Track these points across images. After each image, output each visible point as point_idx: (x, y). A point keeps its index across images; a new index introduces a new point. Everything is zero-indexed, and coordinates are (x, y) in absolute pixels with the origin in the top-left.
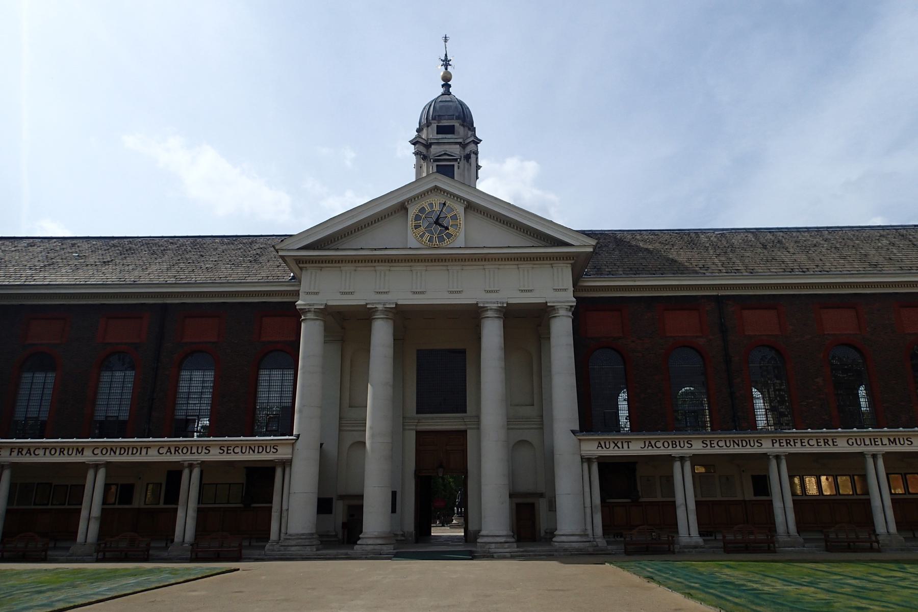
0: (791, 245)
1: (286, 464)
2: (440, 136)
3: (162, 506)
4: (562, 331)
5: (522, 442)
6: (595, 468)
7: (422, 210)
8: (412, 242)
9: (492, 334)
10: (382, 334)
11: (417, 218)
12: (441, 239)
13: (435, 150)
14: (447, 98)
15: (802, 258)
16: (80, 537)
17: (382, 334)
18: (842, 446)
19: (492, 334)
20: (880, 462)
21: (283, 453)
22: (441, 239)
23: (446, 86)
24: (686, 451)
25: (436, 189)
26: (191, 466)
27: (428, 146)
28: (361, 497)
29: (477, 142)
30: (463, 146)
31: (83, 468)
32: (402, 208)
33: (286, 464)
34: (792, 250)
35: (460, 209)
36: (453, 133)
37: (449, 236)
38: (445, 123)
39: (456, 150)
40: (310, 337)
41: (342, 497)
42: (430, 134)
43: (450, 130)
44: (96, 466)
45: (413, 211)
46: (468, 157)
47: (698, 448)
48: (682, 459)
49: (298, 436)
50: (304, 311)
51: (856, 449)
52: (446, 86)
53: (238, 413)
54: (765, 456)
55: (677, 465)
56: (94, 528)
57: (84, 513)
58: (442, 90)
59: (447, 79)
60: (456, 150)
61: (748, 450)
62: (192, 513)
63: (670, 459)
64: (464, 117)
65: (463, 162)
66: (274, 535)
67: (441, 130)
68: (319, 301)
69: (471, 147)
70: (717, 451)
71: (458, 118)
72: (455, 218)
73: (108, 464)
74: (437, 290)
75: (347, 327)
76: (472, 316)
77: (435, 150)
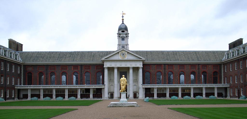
0: (178, 54)
1: (104, 88)
2: (122, 33)
3: (85, 93)
4: (141, 71)
5: (135, 85)
6: (144, 89)
7: (121, 53)
9: (131, 71)
11: (120, 54)
12: (124, 58)
13: (121, 35)
14: (123, 25)
15: (179, 57)
19: (131, 71)
20: (181, 88)
21: (103, 87)
22: (124, 58)
23: (123, 22)
26: (91, 88)
28: (114, 92)
29: (128, 34)
30: (126, 35)
31: (77, 89)
32: (118, 53)
33: (104, 88)
34: (178, 56)
35: (127, 53)
36: (124, 32)
37: (125, 57)
39: (125, 36)
40: (106, 72)
41: (110, 92)
42: (120, 32)
43: (123, 32)
45: (120, 53)
46: (127, 37)
47: (157, 87)
49: (105, 85)
50: (105, 68)
52: (123, 22)
54: (166, 88)
55: (155, 89)
57: (78, 95)
58: (122, 22)
59: (123, 20)
60: (125, 36)
62: (92, 94)
63: (154, 88)
64: (126, 29)
65: (126, 37)
67: (122, 31)
69: (127, 35)
71: (125, 29)
72: (126, 54)
73: (80, 88)
74: (123, 65)
75: (111, 70)
76: (128, 68)
77: (121, 35)
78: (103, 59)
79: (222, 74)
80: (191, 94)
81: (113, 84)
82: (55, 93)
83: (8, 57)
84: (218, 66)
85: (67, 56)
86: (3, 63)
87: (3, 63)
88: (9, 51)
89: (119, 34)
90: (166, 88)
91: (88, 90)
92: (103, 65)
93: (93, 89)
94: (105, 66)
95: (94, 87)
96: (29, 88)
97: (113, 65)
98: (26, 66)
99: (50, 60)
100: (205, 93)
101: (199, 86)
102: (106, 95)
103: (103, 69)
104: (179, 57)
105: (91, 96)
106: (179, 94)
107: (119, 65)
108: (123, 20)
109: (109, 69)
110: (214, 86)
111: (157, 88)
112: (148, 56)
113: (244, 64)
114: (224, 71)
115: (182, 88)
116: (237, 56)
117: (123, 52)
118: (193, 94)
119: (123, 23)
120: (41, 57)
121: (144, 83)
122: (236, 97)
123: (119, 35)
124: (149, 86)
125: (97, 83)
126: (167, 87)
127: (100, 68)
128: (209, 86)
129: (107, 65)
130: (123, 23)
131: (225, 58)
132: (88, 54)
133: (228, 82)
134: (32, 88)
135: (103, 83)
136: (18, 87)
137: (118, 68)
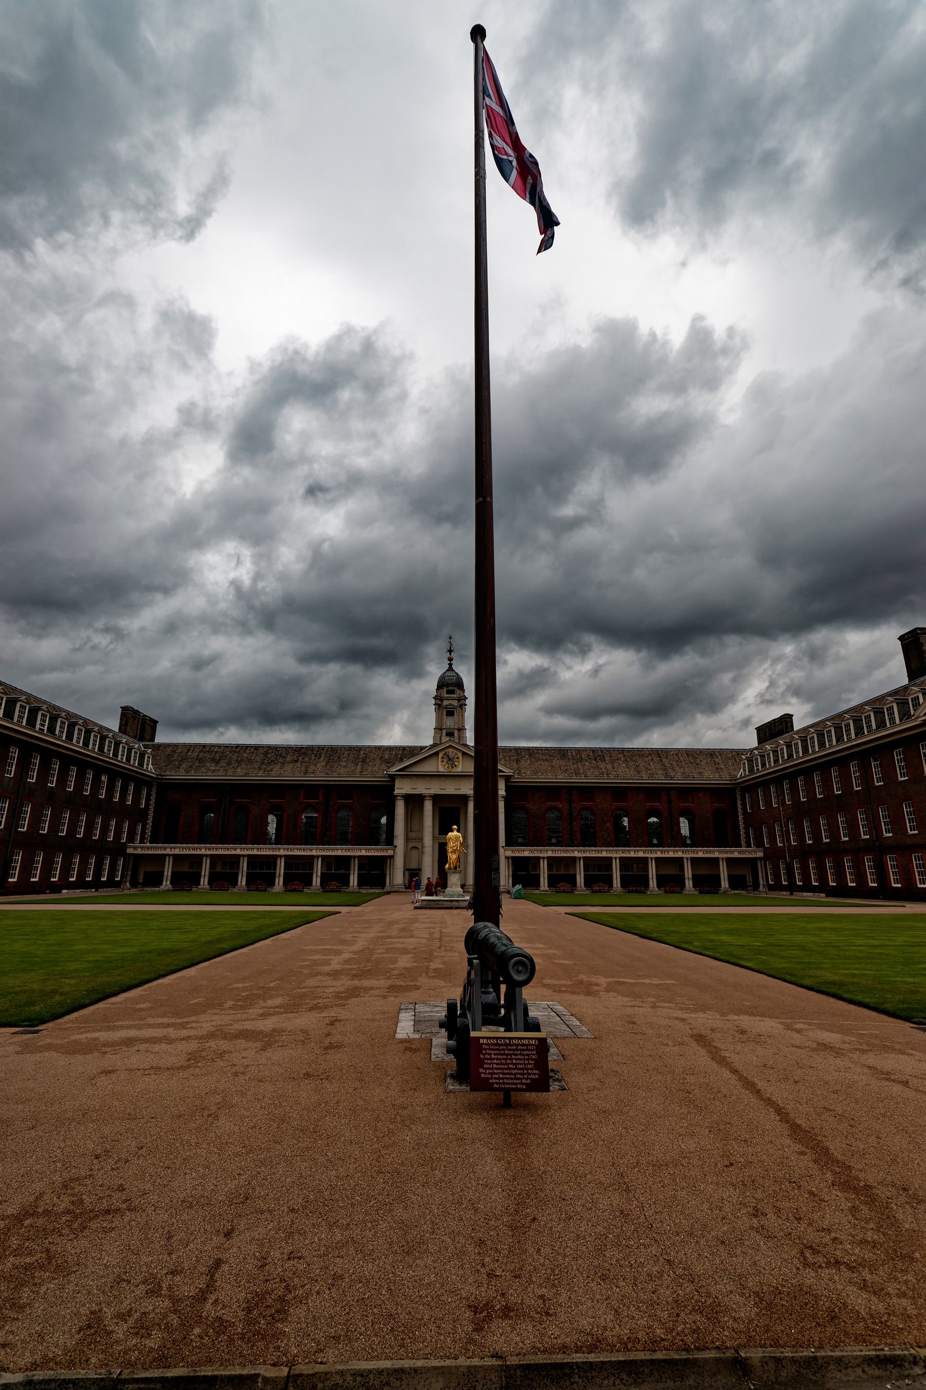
1: (392, 857)
8: (441, 769)
10: (428, 805)
13: (445, 703)
16: (314, 884)
17: (428, 805)
18: (604, 854)
21: (390, 853)
23: (450, 665)
24: (545, 855)
25: (450, 746)
27: (442, 700)
30: (459, 700)
32: (437, 754)
33: (392, 857)
35: (460, 755)
38: (450, 688)
39: (455, 703)
40: (400, 808)
43: (452, 692)
44: (318, 857)
45: (441, 755)
46: (461, 706)
47: (550, 854)
48: (544, 858)
51: (609, 855)
52: (450, 665)
53: (370, 836)
56: (319, 880)
57: (315, 875)
60: (455, 703)
61: (569, 855)
62: (356, 875)
63: (539, 858)
66: (388, 884)
67: (448, 692)
68: (404, 792)
69: (461, 702)
70: (557, 855)
73: (322, 856)
75: (414, 802)
77: (445, 703)
78: (393, 770)
79: (741, 818)
80: (650, 876)
81: (418, 845)
82: (245, 868)
83: (60, 738)
84: (724, 795)
85: (289, 758)
86: (15, 752)
87: (15, 752)
88: (28, 703)
89: (439, 699)
90: (574, 860)
91: (345, 862)
92: (392, 788)
93: (360, 857)
94: (396, 792)
95: (363, 853)
96: (168, 851)
97: (420, 788)
98: (164, 787)
99: (239, 770)
100: (690, 876)
101: (671, 855)
102: (398, 877)
103: (392, 799)
104: (610, 767)
105: (354, 880)
106: (614, 876)
107: (436, 788)
108: (450, 659)
109: (408, 798)
110: (716, 855)
111: (549, 858)
112: (523, 762)
113: (914, 765)
114: (744, 809)
115: (621, 858)
116: (801, 758)
117: (450, 750)
118: (655, 876)
119: (450, 668)
120: (213, 760)
121: (509, 843)
122: (784, 888)
123: (439, 702)
124: (526, 852)
125: (371, 839)
126: (576, 854)
127: (382, 796)
128: (701, 855)
129: (402, 788)
130: (450, 668)
131: (744, 770)
132: (349, 755)
133: (759, 844)
134: (177, 852)
135: (390, 841)
136: (136, 849)
137: (436, 798)
